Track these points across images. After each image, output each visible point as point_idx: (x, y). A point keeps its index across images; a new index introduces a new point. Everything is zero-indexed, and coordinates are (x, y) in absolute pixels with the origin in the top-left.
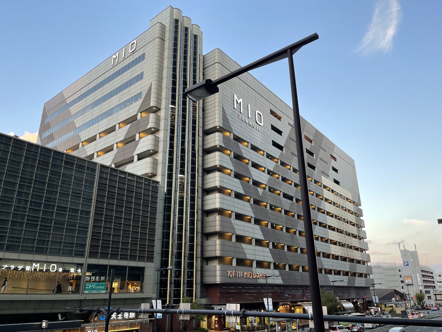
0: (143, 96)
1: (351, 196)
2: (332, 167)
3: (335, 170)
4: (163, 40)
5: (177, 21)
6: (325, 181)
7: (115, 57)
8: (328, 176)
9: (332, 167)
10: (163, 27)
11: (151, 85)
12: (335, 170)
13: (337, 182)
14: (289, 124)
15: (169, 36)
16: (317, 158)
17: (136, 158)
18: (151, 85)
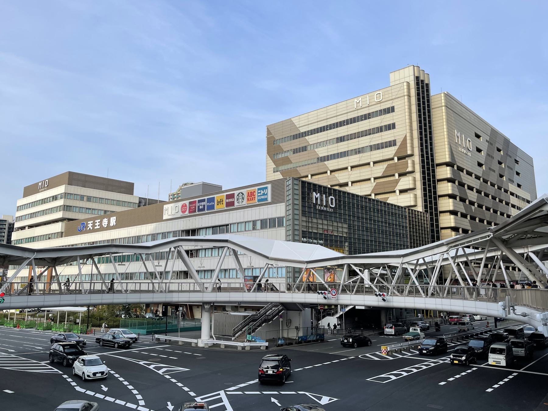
0: (398, 144)
1: (530, 197)
2: (516, 171)
3: (518, 174)
4: (409, 96)
5: (417, 78)
6: (512, 188)
7: (358, 102)
8: (513, 181)
9: (516, 171)
10: (408, 83)
11: (406, 136)
12: (518, 174)
13: (519, 186)
14: (487, 141)
15: (413, 92)
16: (505, 166)
17: (398, 192)
18: (406, 136)
